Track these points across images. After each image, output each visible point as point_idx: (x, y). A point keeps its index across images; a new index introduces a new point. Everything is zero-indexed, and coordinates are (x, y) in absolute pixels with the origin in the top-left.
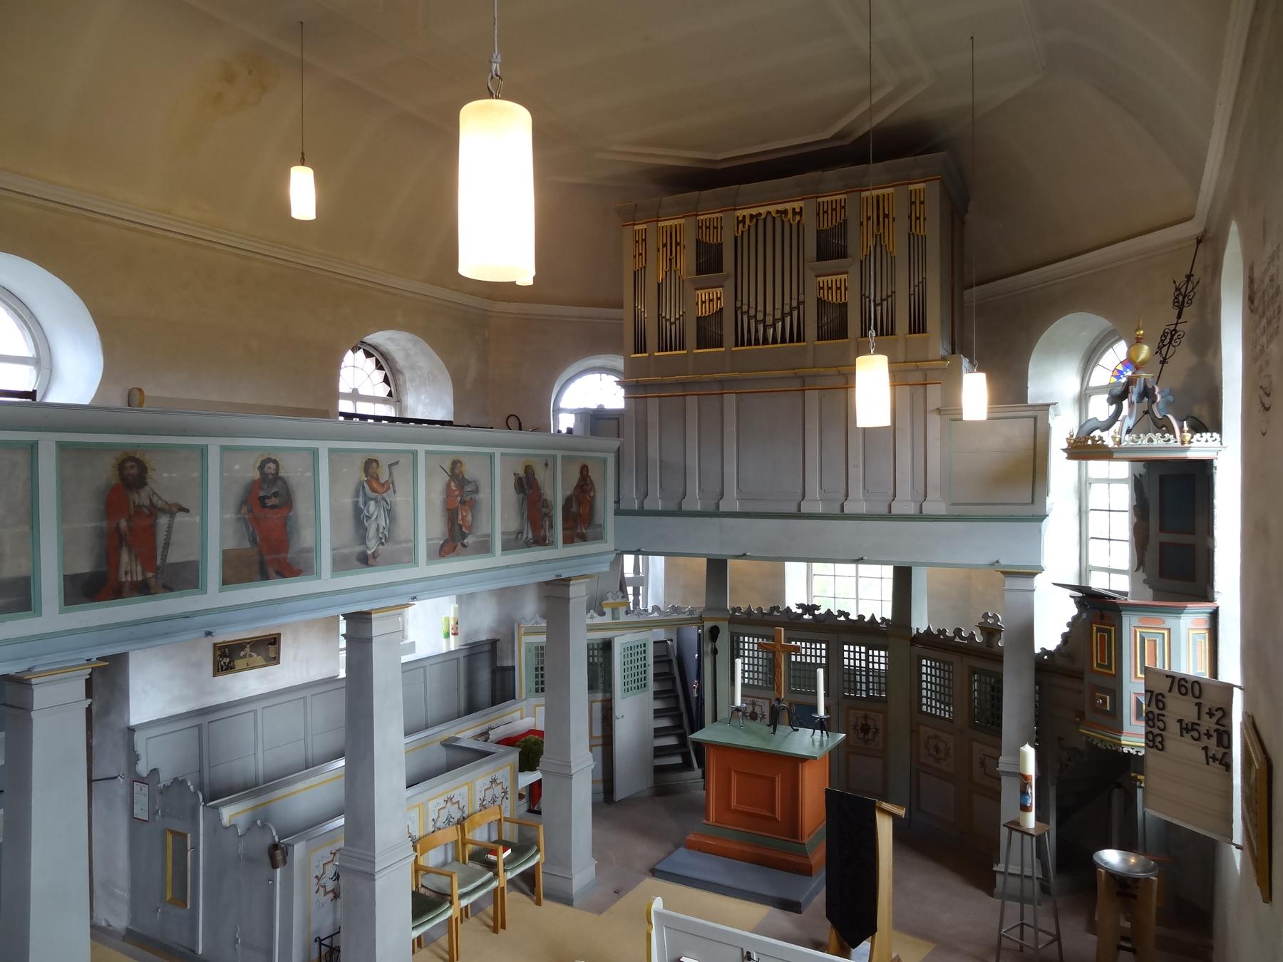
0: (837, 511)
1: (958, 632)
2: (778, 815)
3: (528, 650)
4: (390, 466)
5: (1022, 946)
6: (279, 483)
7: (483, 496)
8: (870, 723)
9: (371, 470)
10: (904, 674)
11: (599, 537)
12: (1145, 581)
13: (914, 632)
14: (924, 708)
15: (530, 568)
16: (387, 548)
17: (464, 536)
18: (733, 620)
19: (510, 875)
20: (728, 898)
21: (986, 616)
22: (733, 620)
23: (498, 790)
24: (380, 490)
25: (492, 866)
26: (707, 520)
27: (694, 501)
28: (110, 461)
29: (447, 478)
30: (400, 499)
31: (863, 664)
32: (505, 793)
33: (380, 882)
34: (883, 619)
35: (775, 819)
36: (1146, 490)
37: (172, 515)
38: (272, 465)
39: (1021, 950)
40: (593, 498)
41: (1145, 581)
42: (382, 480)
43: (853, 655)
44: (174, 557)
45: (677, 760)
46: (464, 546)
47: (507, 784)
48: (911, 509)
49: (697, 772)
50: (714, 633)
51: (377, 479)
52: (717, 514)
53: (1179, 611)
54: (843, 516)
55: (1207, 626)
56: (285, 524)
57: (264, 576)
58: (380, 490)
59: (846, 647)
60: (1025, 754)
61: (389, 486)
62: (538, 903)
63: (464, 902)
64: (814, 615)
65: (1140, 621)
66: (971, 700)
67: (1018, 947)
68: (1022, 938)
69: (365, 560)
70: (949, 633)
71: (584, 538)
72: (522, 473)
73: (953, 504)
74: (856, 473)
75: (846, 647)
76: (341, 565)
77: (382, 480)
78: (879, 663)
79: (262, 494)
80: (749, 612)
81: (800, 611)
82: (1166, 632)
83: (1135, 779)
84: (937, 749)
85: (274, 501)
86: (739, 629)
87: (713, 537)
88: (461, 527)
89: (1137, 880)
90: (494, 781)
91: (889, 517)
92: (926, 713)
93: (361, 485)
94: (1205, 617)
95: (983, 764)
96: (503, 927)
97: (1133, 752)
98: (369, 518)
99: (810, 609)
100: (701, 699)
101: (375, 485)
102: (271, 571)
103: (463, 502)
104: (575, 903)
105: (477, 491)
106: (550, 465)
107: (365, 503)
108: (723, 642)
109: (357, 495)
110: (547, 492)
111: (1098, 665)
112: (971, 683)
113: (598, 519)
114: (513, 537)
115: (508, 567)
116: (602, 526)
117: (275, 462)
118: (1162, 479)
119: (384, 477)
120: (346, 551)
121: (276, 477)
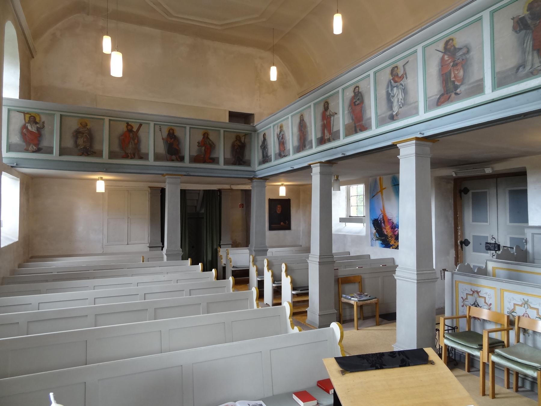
4: (404, 66)
6: (360, 94)
7: (474, 54)
9: (394, 73)
16: (404, 109)
17: (456, 87)
28: (322, 104)
29: (441, 55)
30: (409, 82)
37: (334, 116)
38: (357, 88)
42: (400, 75)
44: (335, 129)
46: (457, 94)
56: (361, 110)
57: (356, 132)
61: (405, 76)
69: (392, 118)
76: (381, 122)
77: (400, 75)
79: (354, 101)
85: (358, 102)
88: (454, 82)
101: (396, 79)
102: (358, 130)
103: (455, 65)
105: (468, 52)
107: (392, 90)
109: (388, 87)
117: (358, 87)
119: (401, 72)
120: (383, 116)
121: (359, 92)
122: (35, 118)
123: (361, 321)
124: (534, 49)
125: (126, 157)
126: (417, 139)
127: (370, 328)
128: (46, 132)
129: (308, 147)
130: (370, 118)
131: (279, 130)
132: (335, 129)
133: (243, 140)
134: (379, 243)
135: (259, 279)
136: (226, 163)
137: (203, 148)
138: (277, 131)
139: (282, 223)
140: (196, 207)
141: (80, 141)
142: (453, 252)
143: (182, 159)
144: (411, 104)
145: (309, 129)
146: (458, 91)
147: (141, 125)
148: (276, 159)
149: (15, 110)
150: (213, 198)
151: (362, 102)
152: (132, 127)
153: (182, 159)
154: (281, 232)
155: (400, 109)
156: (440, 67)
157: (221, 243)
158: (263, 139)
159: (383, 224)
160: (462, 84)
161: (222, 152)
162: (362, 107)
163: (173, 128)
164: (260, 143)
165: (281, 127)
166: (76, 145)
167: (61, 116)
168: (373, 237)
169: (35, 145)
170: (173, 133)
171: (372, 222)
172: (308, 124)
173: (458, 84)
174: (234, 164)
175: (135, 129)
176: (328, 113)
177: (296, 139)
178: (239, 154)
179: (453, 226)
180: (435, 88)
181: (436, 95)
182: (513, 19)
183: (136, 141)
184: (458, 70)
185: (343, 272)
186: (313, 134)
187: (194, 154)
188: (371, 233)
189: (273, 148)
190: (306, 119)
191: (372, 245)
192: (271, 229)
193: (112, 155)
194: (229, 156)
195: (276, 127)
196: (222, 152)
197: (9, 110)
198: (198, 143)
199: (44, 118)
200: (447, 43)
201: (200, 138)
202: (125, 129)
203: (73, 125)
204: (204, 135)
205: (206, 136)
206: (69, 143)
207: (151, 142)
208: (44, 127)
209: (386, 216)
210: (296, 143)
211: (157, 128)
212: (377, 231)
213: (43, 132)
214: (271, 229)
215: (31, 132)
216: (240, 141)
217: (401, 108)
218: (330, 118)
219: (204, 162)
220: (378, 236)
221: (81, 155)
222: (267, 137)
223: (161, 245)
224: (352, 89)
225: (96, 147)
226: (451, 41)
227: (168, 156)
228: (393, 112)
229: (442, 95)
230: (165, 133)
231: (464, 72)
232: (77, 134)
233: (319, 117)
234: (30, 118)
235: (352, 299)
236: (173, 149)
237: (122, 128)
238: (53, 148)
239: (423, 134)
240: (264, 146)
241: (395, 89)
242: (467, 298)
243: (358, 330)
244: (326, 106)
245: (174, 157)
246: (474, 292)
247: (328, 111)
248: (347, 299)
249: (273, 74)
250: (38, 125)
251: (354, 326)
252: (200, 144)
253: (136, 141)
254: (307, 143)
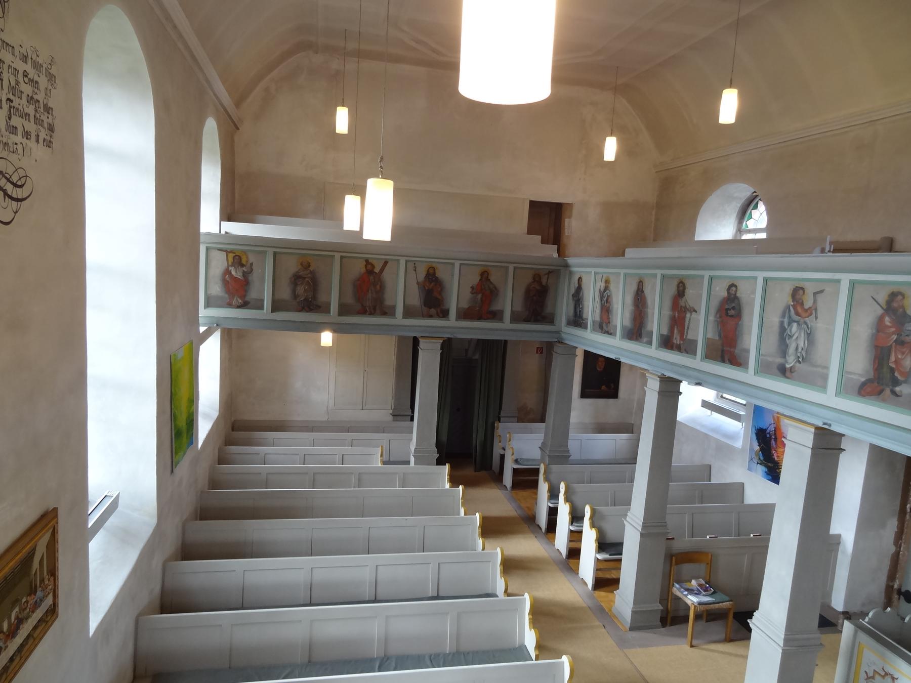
4: (815, 294)
9: (798, 297)
17: (896, 382)
24: (804, 314)
28: (675, 283)
29: (880, 311)
30: (819, 325)
37: (691, 313)
38: (734, 289)
42: (806, 307)
44: (690, 336)
46: (894, 393)
51: (802, 304)
57: (723, 361)
58: (804, 314)
61: (812, 311)
69: (784, 372)
76: (764, 368)
77: (806, 307)
79: (727, 307)
85: (732, 312)
88: (892, 370)
93: (788, 307)
98: (790, 337)
101: (799, 309)
103: (900, 343)
107: (789, 324)
109: (783, 316)
117: (736, 286)
119: (808, 303)
120: (770, 359)
122: (240, 258)
123: (702, 624)
125: (363, 312)
126: (818, 428)
127: (713, 646)
128: (254, 277)
129: (645, 340)
130: (748, 351)
131: (603, 285)
132: (690, 336)
133: (544, 281)
134: (761, 469)
135: (551, 505)
136: (515, 318)
137: (479, 296)
138: (601, 285)
139: (603, 387)
140: (467, 351)
141: (300, 290)
142: (892, 525)
143: (445, 314)
144: (816, 366)
145: (649, 311)
146: (897, 389)
147: (386, 263)
148: (593, 330)
149: (214, 248)
150: (494, 352)
151: (738, 315)
152: (373, 266)
153: (445, 314)
154: (601, 402)
155: (798, 364)
157: (502, 414)
158: (577, 285)
159: (773, 442)
160: (905, 382)
161: (509, 301)
162: (737, 325)
163: (434, 265)
164: (573, 291)
165: (607, 282)
166: (295, 296)
167: (275, 254)
168: (754, 456)
169: (241, 298)
170: (434, 273)
171: (754, 431)
172: (649, 302)
173: (899, 377)
174: (527, 320)
175: (377, 270)
176: (682, 303)
177: (628, 315)
178: (538, 298)
179: (902, 478)
180: (861, 365)
181: (860, 375)
183: (378, 287)
184: (903, 353)
185: (684, 543)
186: (656, 323)
187: (465, 305)
188: (751, 449)
189: (591, 309)
190: (647, 291)
191: (749, 469)
192: (584, 395)
193: (344, 310)
194: (519, 307)
195: (599, 277)
196: (509, 301)
197: (207, 249)
198: (472, 288)
199: (252, 259)
200: (893, 296)
201: (475, 279)
202: (363, 270)
203: (291, 266)
204: (482, 274)
205: (485, 276)
206: (285, 293)
207: (401, 289)
208: (252, 270)
209: (780, 430)
210: (628, 323)
211: (411, 265)
212: (762, 449)
213: (250, 278)
214: (584, 395)
215: (236, 279)
216: (540, 283)
217: (800, 362)
218: (685, 312)
219: (480, 317)
220: (762, 458)
221: (300, 311)
222: (584, 286)
223: (410, 413)
224: (726, 285)
225: (322, 298)
226: (900, 297)
227: (425, 309)
228: (786, 362)
230: (422, 276)
232: (296, 279)
233: (668, 303)
234: (234, 258)
235: (690, 597)
236: (432, 298)
237: (359, 268)
238: (263, 301)
239: (830, 425)
240: (578, 297)
241: (795, 325)
242: (873, 677)
243: (692, 646)
244: (681, 291)
245: (433, 311)
246: (886, 674)
247: (684, 299)
248: (682, 592)
249: (611, 148)
250: (244, 269)
251: (685, 636)
252: (474, 290)
253: (378, 287)
254: (643, 332)
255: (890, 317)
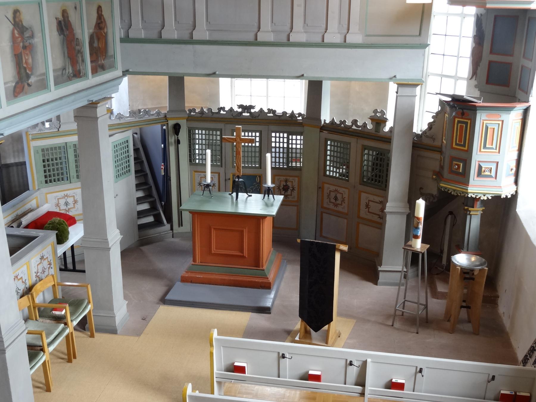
0: (285, 40)
1: (355, 122)
2: (246, 253)
3: (36, 152)
5: (403, 312)
7: (37, 40)
8: (289, 184)
10: (315, 152)
11: (112, 67)
12: (476, 86)
13: (323, 123)
14: (328, 173)
15: (72, 98)
17: (28, 77)
18: (190, 119)
19: (75, 323)
20: (220, 311)
21: (375, 111)
22: (190, 119)
23: (45, 263)
25: (59, 319)
26: (183, 46)
27: (171, 31)
29: (12, 27)
31: (285, 145)
32: (50, 264)
33: (9, 354)
34: (300, 114)
35: (243, 257)
36: (484, 25)
39: (403, 315)
40: (106, 34)
41: (476, 86)
43: (278, 139)
45: (150, 219)
46: (29, 85)
47: (51, 258)
48: (338, 39)
49: (167, 226)
50: (177, 128)
52: (191, 41)
53: (510, 109)
54: (289, 44)
55: (521, 117)
59: (273, 134)
60: (419, 205)
62: (92, 336)
63: (51, 348)
64: (250, 113)
65: (487, 116)
66: (362, 166)
67: (401, 313)
68: (403, 309)
70: (349, 123)
71: (103, 68)
72: (60, 17)
73: (367, 36)
74: (298, 11)
75: (273, 134)
78: (296, 144)
80: (202, 112)
81: (240, 110)
82: (500, 123)
83: (467, 210)
84: (336, 198)
86: (194, 124)
87: (181, 59)
88: (25, 69)
89: (472, 270)
90: (42, 258)
91: (323, 44)
92: (329, 176)
94: (521, 112)
95: (367, 206)
96: (75, 357)
97: (474, 196)
99: (247, 108)
100: (167, 177)
103: (25, 47)
104: (118, 332)
105: (32, 36)
106: (78, 7)
108: (183, 135)
110: (78, 31)
111: (456, 144)
112: (362, 155)
113: (110, 52)
114: (60, 73)
115: (61, 98)
116: (114, 56)
118: (496, 17)
124: (68, 57)
156: (12, 44)
181: (12, 82)
182: (56, 18)
184: (27, 54)
229: (17, 83)
231: (32, 58)
255: (17, 30)
